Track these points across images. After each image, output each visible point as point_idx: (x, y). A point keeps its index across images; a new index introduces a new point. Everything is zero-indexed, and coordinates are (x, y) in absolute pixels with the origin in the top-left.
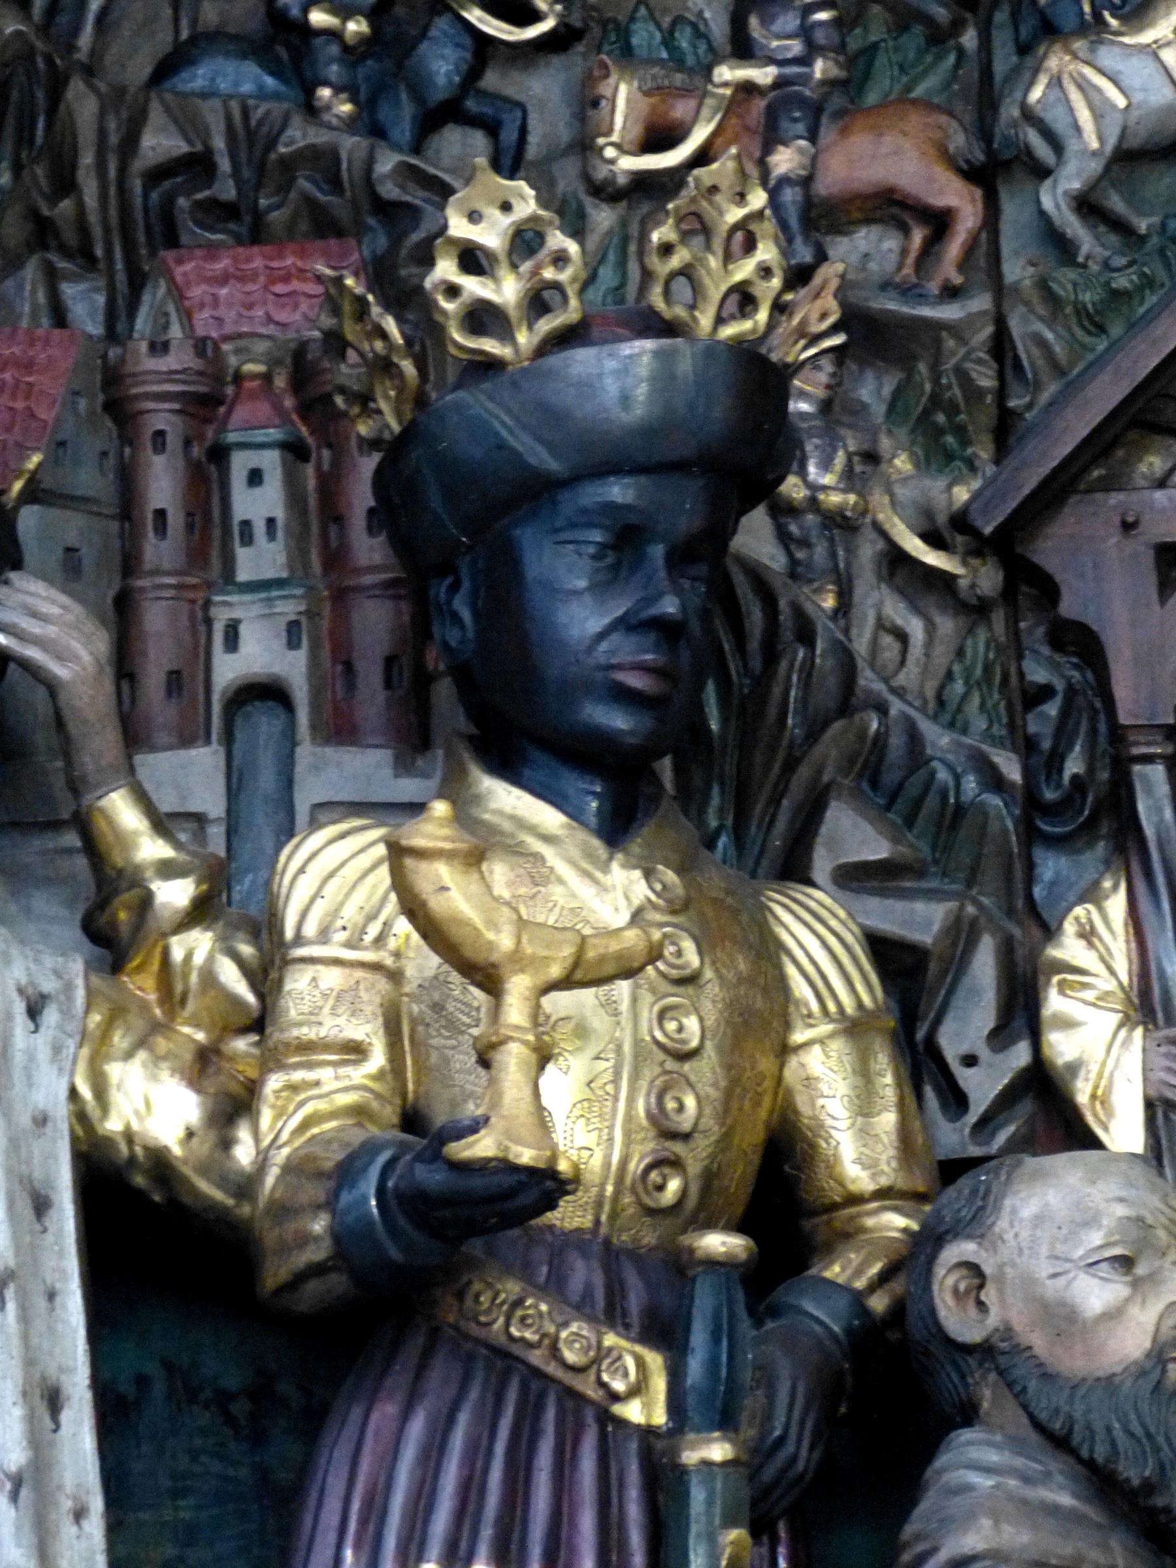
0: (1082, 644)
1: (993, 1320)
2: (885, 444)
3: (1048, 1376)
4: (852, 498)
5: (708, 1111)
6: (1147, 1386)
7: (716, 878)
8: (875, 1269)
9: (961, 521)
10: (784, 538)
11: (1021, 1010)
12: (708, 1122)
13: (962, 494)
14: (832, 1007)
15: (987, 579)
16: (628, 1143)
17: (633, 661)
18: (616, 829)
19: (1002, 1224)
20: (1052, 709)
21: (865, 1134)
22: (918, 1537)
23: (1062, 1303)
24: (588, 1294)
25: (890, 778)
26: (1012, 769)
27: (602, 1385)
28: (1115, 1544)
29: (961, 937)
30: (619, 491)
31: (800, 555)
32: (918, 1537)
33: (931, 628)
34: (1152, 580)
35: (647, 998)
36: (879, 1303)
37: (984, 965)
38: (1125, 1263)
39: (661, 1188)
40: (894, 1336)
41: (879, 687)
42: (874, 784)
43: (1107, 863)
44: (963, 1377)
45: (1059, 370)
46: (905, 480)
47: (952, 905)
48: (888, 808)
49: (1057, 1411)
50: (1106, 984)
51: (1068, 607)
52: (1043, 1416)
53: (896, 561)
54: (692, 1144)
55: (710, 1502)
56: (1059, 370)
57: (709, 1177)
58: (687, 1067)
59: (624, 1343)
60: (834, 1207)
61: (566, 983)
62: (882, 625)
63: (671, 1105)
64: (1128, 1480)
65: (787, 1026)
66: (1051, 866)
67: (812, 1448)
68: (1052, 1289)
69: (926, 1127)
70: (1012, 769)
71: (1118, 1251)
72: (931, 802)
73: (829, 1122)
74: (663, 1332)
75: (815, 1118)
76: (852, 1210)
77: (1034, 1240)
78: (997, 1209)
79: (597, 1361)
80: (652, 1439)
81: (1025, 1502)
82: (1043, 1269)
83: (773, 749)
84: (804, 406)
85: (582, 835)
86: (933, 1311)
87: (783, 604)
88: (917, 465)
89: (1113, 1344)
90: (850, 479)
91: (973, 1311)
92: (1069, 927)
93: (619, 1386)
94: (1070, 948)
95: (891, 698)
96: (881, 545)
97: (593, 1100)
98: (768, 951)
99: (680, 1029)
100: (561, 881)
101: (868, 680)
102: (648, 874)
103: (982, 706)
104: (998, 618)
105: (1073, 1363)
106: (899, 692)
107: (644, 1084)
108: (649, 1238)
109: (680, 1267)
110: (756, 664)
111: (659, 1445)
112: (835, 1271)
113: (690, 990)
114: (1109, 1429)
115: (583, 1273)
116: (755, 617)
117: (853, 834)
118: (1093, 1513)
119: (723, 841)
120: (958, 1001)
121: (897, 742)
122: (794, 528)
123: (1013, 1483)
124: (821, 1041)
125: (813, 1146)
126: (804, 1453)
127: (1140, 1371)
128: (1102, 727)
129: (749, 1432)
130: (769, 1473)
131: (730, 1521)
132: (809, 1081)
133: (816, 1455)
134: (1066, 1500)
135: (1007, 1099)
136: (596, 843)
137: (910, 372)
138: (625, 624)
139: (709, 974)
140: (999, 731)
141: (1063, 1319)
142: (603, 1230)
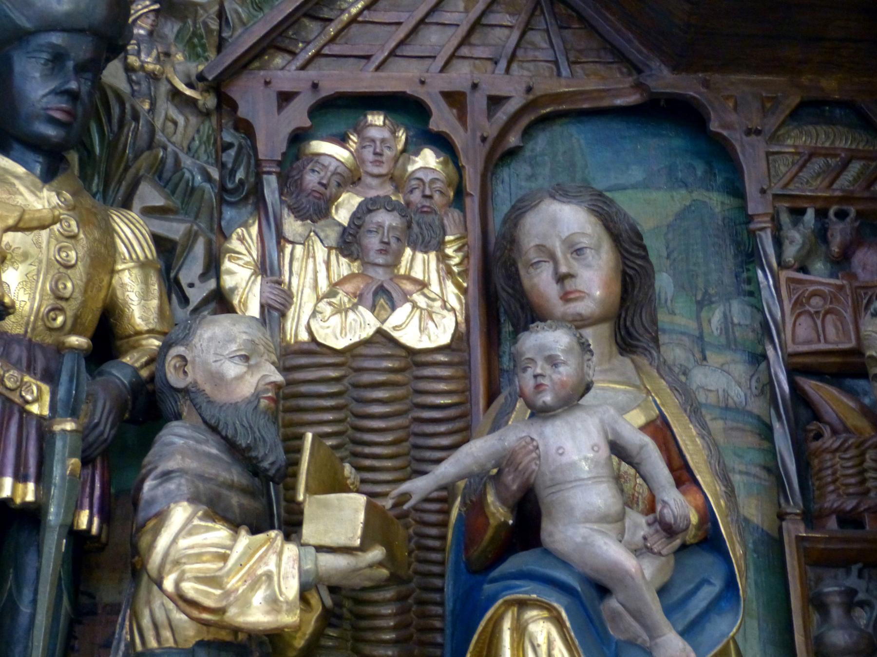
0: (246, 128)
1: (189, 379)
2: (173, 49)
3: (210, 402)
4: (158, 67)
5: (77, 290)
6: (251, 407)
7: (87, 201)
8: (144, 360)
9: (201, 77)
10: (130, 81)
11: (213, 267)
12: (77, 294)
13: (201, 68)
14: (134, 256)
15: (210, 101)
16: (41, 300)
17: (58, 107)
18: (48, 176)
19: (196, 340)
20: (232, 152)
21: (145, 308)
22: (149, 463)
23: (218, 373)
24: (20, 359)
25: (166, 175)
26: (215, 174)
27: (22, 397)
28: (234, 471)
29: (191, 238)
30: (56, 39)
31: (136, 88)
32: (149, 463)
33: (187, 120)
34: (275, 104)
35: (53, 242)
36: (144, 373)
37: (199, 249)
38: (246, 358)
39: (55, 319)
40: (150, 387)
41: (164, 139)
42: (160, 178)
43: (251, 214)
44: (176, 402)
45: (244, 24)
46: (180, 63)
47: (188, 225)
48: (165, 187)
49: (213, 416)
50: (248, 259)
51: (242, 112)
52: (207, 418)
53: (175, 94)
54: (69, 303)
55: (64, 447)
56: (244, 24)
57: (77, 318)
58: (69, 272)
59: (33, 380)
60: (130, 336)
61: (15, 228)
62: (167, 118)
63: (61, 286)
64: (241, 445)
65: (115, 262)
66: (229, 213)
67: (111, 429)
68: (214, 366)
69: (171, 310)
70: (215, 174)
71: (243, 353)
72: (182, 185)
73: (130, 301)
74: (50, 377)
75: (124, 300)
76: (137, 337)
77: (208, 347)
78: (194, 333)
79: (20, 387)
80: (42, 420)
81: (196, 450)
82: (211, 358)
83: (120, 162)
84: (142, 32)
85: (32, 177)
86: (165, 375)
87: (128, 106)
88: (185, 58)
89: (238, 390)
90: (158, 60)
91: (181, 375)
92: (234, 236)
93: (29, 397)
94: (235, 244)
95: (169, 144)
96: (169, 87)
97: (29, 282)
98: (109, 232)
99: (68, 256)
100: (21, 194)
101: (160, 137)
102: (59, 194)
103: (206, 151)
104: (214, 119)
105: (221, 397)
106: (173, 144)
107: (50, 277)
108: (49, 340)
109: (60, 349)
110: (115, 128)
111: (45, 423)
112: (127, 359)
113: (73, 241)
114: (234, 424)
115: (17, 352)
116: (116, 111)
117: (150, 195)
118: (224, 457)
119: (98, 196)
120: (188, 262)
121: (170, 161)
122: (134, 77)
123: (191, 442)
124: (129, 269)
125: (123, 311)
126: (107, 430)
127: (248, 401)
128: (253, 161)
129: (84, 420)
130: (91, 438)
131: (72, 455)
132: (123, 285)
133: (113, 432)
134: (214, 451)
135: (206, 301)
136: (38, 182)
137: (185, 23)
138: (55, 92)
139: (82, 236)
140: (212, 160)
141: (218, 379)
142: (29, 335)
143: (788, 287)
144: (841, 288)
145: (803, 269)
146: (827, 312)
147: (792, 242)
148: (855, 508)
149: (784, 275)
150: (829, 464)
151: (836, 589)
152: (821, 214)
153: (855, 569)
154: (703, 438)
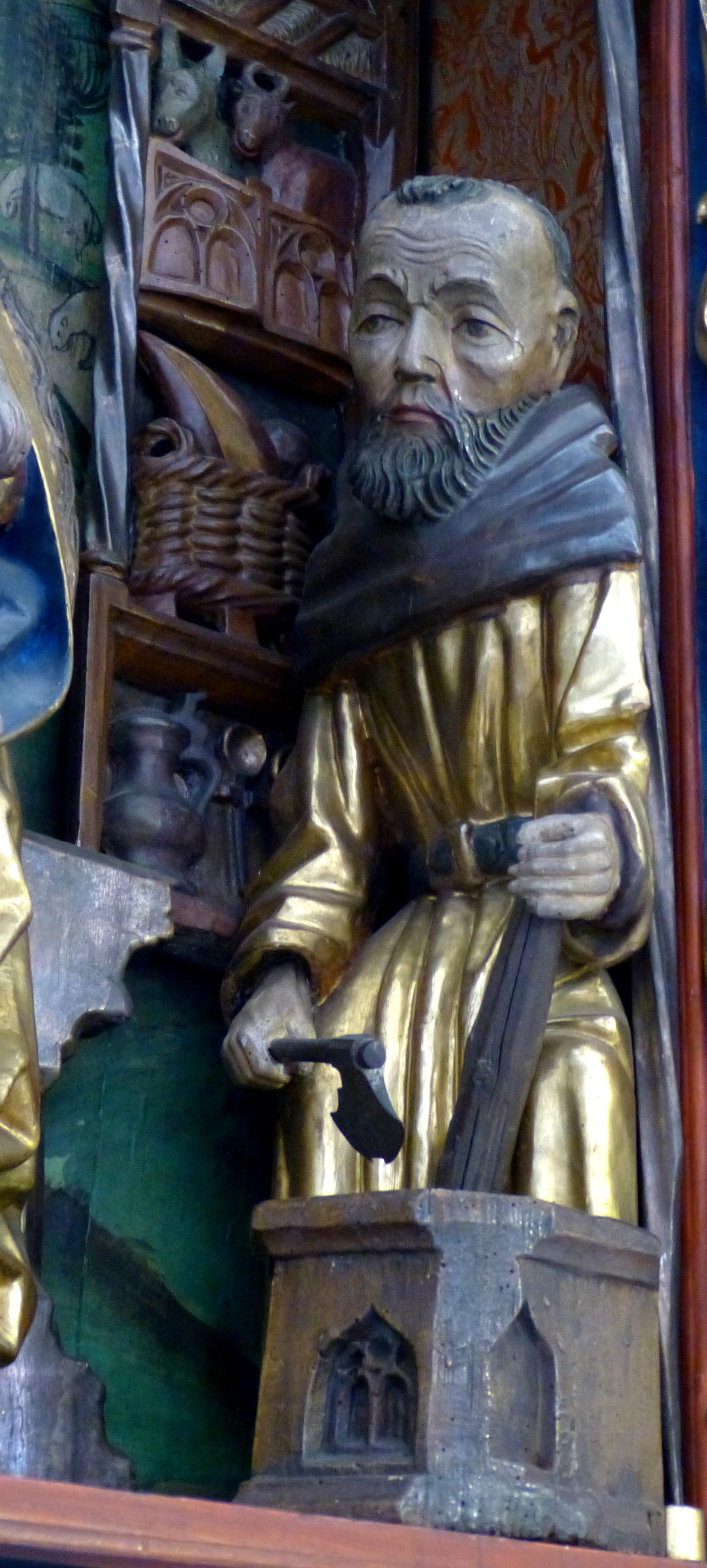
143: (159, 170)
144: (248, 203)
145: (184, 147)
146: (219, 236)
147: (180, 91)
148: (208, 592)
149: (156, 144)
150: (178, 500)
151: (164, 723)
152: (233, 69)
153: (191, 700)
154: (26, 342)
